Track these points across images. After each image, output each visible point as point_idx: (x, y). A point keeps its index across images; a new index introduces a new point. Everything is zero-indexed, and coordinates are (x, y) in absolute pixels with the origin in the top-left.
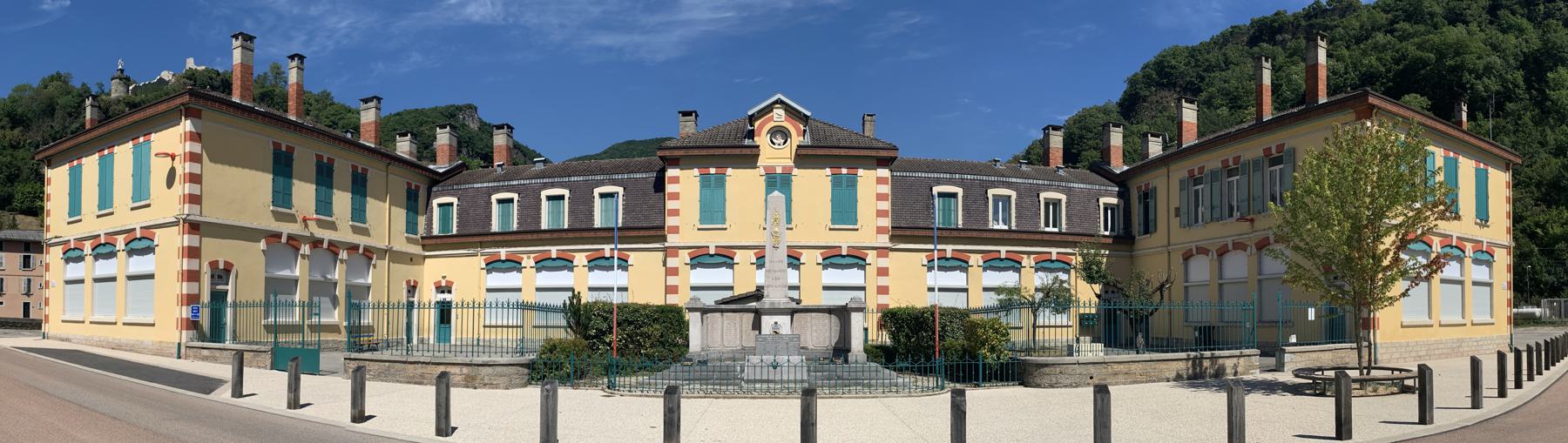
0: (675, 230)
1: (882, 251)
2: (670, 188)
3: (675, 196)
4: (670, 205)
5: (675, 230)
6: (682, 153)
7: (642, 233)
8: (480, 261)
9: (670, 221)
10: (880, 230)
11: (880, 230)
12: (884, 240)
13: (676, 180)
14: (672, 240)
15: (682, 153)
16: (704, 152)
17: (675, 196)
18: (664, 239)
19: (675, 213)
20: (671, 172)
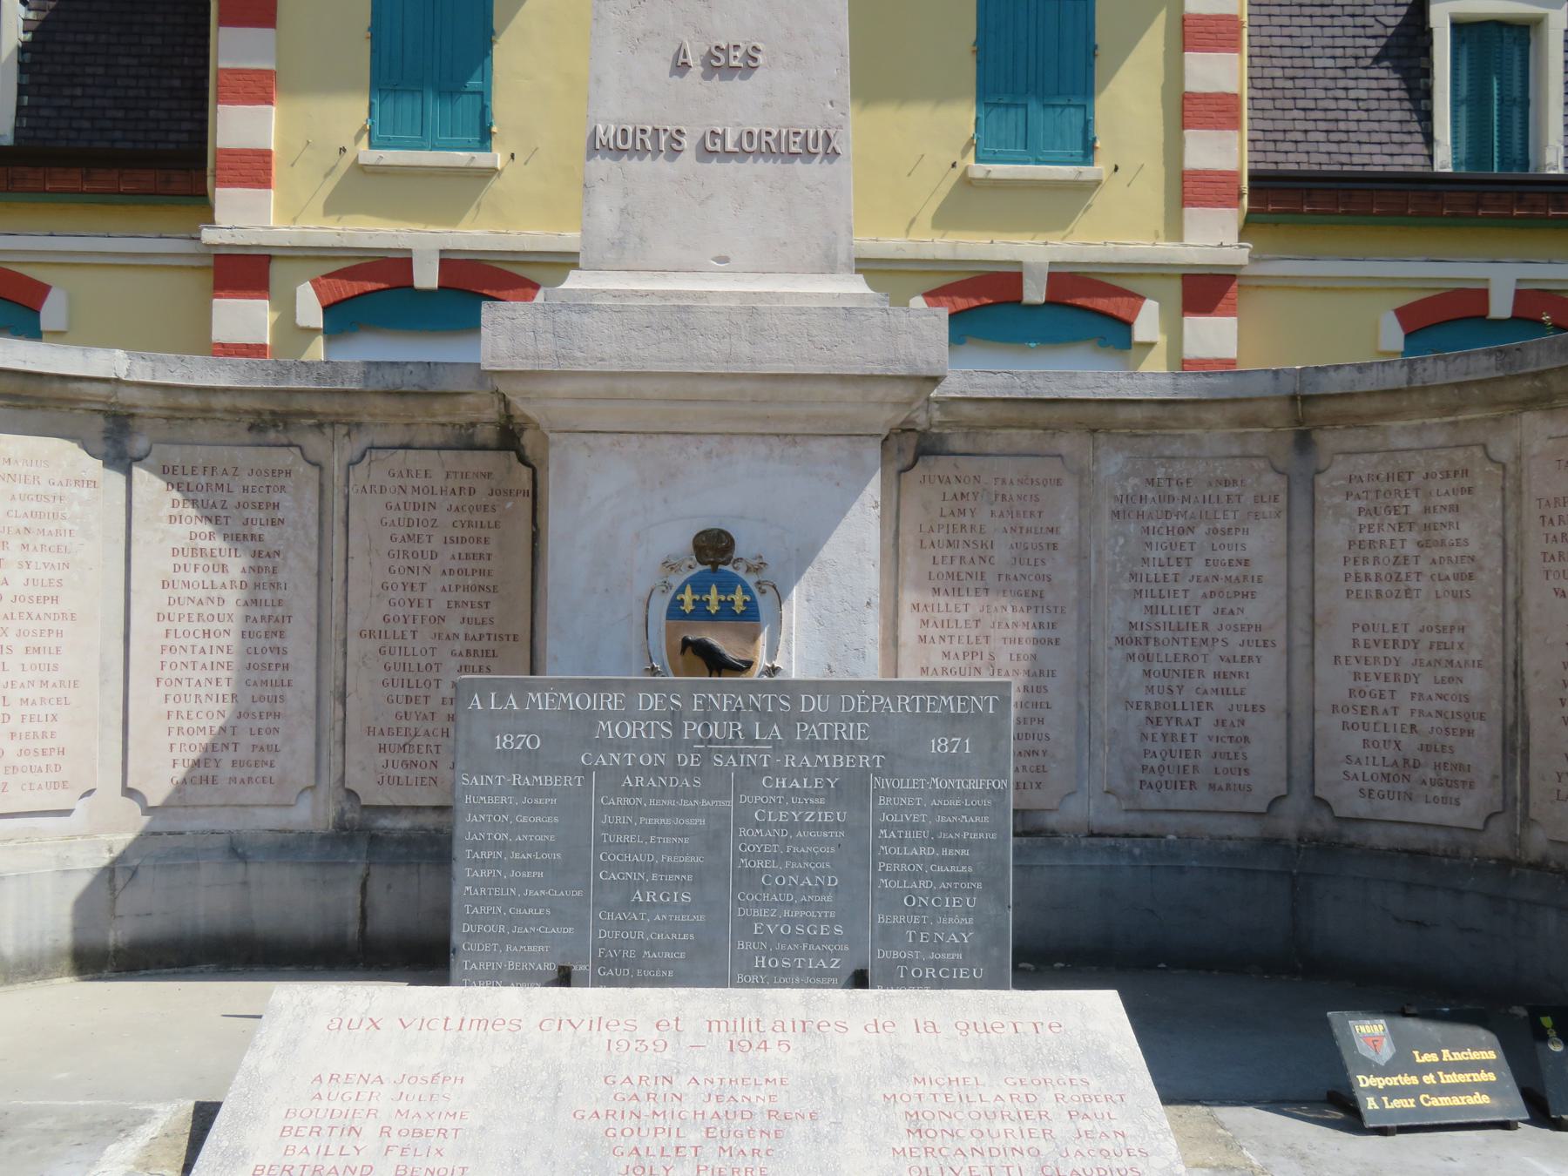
0: (254, 169)
1: (1204, 291)
5: (254, 169)
9: (233, 126)
10: (1193, 190)
11: (1193, 190)
12: (1215, 237)
14: (239, 218)
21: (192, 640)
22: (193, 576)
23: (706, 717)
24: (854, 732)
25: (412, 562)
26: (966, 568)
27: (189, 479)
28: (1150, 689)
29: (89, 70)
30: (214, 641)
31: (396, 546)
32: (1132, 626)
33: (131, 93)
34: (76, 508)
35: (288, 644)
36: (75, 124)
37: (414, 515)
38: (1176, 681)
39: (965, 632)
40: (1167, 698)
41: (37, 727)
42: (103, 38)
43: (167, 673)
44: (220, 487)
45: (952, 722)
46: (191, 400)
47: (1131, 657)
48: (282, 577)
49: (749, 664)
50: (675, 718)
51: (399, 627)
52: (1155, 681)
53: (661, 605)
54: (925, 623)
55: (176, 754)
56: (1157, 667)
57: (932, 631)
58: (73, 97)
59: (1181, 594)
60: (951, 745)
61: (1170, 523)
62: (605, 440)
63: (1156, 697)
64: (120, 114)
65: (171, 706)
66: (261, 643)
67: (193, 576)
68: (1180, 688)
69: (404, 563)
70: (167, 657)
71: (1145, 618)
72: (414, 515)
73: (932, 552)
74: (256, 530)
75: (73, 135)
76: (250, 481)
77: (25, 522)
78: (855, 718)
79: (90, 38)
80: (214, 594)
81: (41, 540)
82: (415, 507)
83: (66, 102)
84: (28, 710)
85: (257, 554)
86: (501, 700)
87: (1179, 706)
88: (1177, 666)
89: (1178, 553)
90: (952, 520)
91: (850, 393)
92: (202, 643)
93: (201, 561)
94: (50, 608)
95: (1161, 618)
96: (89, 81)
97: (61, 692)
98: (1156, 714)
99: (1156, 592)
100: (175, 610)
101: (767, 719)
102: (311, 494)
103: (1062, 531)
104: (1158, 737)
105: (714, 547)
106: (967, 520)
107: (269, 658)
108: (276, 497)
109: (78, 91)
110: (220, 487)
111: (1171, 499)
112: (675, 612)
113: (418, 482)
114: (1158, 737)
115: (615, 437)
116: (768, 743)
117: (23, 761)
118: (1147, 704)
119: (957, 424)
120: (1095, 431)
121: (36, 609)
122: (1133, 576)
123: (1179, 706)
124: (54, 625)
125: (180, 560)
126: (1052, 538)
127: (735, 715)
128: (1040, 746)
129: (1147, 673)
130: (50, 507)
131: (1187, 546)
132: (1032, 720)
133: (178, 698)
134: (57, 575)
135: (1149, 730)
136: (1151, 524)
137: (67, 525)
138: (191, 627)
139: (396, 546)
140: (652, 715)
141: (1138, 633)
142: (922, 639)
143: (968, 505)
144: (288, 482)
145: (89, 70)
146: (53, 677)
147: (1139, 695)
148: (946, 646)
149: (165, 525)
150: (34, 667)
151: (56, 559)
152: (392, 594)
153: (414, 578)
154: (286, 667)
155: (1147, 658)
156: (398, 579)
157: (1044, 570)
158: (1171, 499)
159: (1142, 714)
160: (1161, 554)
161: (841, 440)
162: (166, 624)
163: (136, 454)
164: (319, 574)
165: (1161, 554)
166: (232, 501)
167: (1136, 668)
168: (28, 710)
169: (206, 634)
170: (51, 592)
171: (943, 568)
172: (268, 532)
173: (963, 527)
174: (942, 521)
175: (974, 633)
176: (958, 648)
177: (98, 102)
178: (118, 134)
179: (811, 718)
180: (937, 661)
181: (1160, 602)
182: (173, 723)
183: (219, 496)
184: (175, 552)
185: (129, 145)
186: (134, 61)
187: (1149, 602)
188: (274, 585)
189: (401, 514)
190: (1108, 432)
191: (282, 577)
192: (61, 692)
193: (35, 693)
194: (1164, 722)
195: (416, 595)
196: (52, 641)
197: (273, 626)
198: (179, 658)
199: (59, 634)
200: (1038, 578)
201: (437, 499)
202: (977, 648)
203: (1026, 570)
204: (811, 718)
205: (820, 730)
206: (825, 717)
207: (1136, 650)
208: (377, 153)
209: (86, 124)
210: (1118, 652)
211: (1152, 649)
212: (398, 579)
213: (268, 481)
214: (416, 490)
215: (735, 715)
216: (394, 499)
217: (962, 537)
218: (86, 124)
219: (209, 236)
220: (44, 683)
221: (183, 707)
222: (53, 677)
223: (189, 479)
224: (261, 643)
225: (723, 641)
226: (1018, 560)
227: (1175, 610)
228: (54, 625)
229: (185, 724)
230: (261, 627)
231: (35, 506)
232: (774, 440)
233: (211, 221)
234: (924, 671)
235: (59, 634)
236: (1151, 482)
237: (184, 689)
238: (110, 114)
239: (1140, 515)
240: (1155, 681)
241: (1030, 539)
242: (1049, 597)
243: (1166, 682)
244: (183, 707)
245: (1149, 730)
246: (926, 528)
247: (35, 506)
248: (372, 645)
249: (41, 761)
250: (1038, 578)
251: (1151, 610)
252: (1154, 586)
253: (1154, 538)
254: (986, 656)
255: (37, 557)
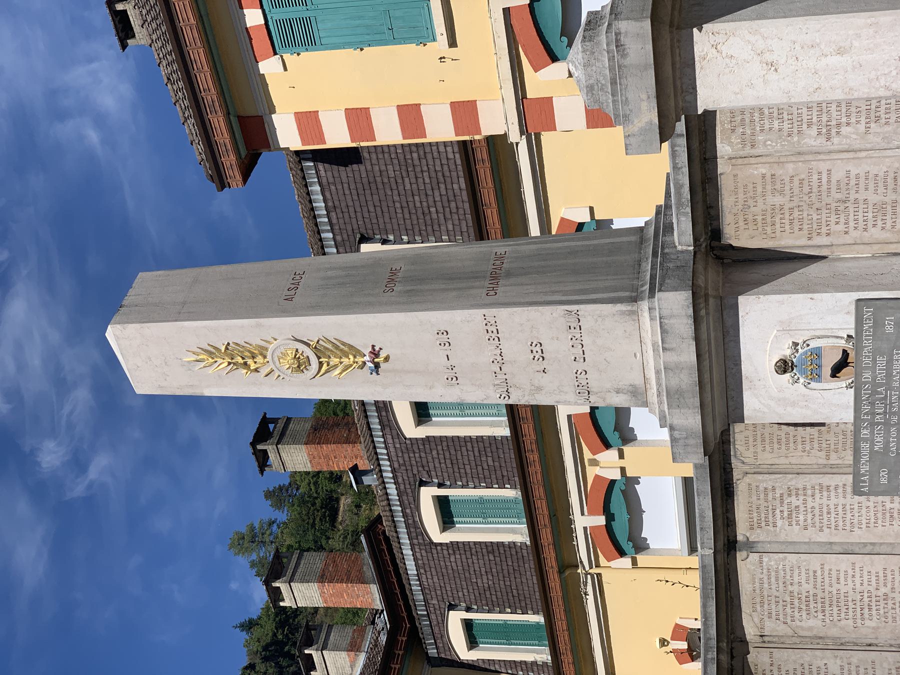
0: (465, 112)
2: (337, 136)
3: (358, 118)
4: (388, 132)
5: (465, 112)
6: (218, 122)
7: (488, 194)
8: (616, 573)
9: (440, 128)
13: (308, 122)
14: (497, 119)
15: (218, 122)
16: (198, 55)
17: (358, 118)
18: (498, 145)
19: (410, 116)
20: (288, 135)
21: (832, 518)
22: (801, 518)
23: (873, 414)
24: (882, 361)
25: (792, 440)
26: (787, 216)
27: (755, 520)
28: (858, 122)
29: (418, 204)
30: (832, 510)
31: (783, 447)
32: (819, 134)
33: (427, 180)
34: (772, 563)
35: (833, 484)
36: (454, 210)
37: (767, 441)
38: (853, 109)
39: (824, 215)
40: (864, 113)
41: (874, 579)
42: (396, 198)
43: (848, 528)
44: (758, 508)
45: (878, 324)
46: (720, 522)
47: (838, 133)
48: (800, 486)
49: (845, 351)
50: (873, 424)
51: (824, 445)
52: (853, 120)
53: (813, 385)
54: (819, 234)
55: (887, 524)
56: (844, 120)
57: (824, 230)
58: (437, 212)
59: (800, 111)
60: (889, 324)
61: (757, 120)
62: (730, 403)
63: (863, 119)
64: (442, 186)
65: (864, 526)
66: (833, 494)
67: (801, 518)
68: (857, 107)
69: (792, 445)
70: (840, 528)
71: (815, 127)
72: (767, 441)
73: (778, 234)
74: (778, 495)
75: (461, 211)
76: (754, 498)
77: (781, 584)
78: (874, 361)
79: (398, 205)
80: (809, 510)
81: (788, 577)
82: (763, 440)
83: (441, 216)
84: (865, 583)
85: (790, 495)
86: (864, 482)
87: (868, 107)
88: (844, 110)
89: (775, 114)
90: (760, 224)
91: (704, 327)
92: (833, 515)
93: (794, 515)
94: (819, 573)
95: (815, 119)
96: (425, 204)
97: (857, 569)
98: (873, 118)
99: (799, 123)
100: (818, 524)
101: (874, 392)
102: (760, 477)
103: (764, 171)
104: (887, 116)
105: (784, 366)
106: (759, 218)
107: (840, 490)
108: (761, 488)
109: (433, 210)
110: (758, 508)
111: (743, 120)
112: (818, 377)
113: (751, 440)
114: (887, 116)
115: (729, 400)
116: (886, 392)
117: (889, 585)
118: (867, 123)
119: (706, 226)
120: (705, 159)
121: (819, 580)
122: (789, 135)
123: (868, 107)
124: (826, 573)
125: (794, 523)
126: (768, 176)
127: (872, 404)
128: (891, 175)
129: (848, 124)
130: (773, 574)
131: (771, 111)
132: (875, 180)
133: (860, 523)
134: (803, 570)
135: (883, 121)
136: (758, 129)
137: (781, 567)
138: (826, 519)
139: (783, 447)
140: (872, 433)
141: (824, 130)
142: (828, 234)
143: (750, 217)
144: (754, 485)
145: (418, 204)
146: (850, 572)
147: (862, 127)
148: (832, 223)
149: (778, 529)
150: (846, 580)
151: (796, 572)
152: (808, 448)
153: (800, 440)
154: (845, 485)
155: (839, 125)
156: (800, 447)
157: (787, 179)
158: (743, 120)
159: (873, 125)
160: (776, 124)
161: (725, 313)
162: (825, 528)
163: (745, 539)
164: (798, 474)
165: (776, 124)
166: (766, 504)
167: (845, 130)
168: (865, 583)
169: (829, 513)
170: (811, 574)
171: (787, 227)
172: (778, 493)
173: (763, 219)
174: (760, 229)
175: (824, 211)
176: (833, 218)
177: (438, 199)
178: (456, 186)
179: (874, 378)
180: (841, 227)
181: (805, 121)
182: (872, 525)
183: (762, 508)
184: (790, 525)
185: (462, 180)
186: (407, 180)
187: (805, 126)
188: (805, 489)
189: (767, 446)
190: (705, 153)
191: (800, 486)
192: (857, 569)
193: (858, 581)
194: (878, 114)
195: (808, 440)
196: (834, 573)
197: (825, 489)
198: (841, 524)
199: (830, 570)
200: (791, 181)
201: (759, 433)
202: (833, 209)
203: (787, 188)
204: (874, 378)
205: (880, 374)
206: (874, 372)
207: (834, 131)
208: (438, 37)
209: (453, 205)
210: (836, 140)
211: (834, 123)
212: (800, 447)
213: (754, 491)
214: (755, 441)
215: (872, 404)
216: (759, 448)
217: (769, 220)
218: (453, 205)
219: (514, 136)
220: (853, 576)
221: (864, 522)
222: (850, 572)
223: (755, 520)
224: (833, 494)
225: (831, 359)
226: (782, 193)
227: (810, 113)
228: (826, 573)
229: (873, 520)
230: (825, 494)
231: (773, 580)
232: (726, 340)
233: (505, 136)
234: (846, 233)
235: (830, 570)
236: (733, 131)
237: (856, 521)
238: (444, 192)
239: (753, 134)
240: (853, 120)
241: (769, 187)
242: (803, 176)
243: (854, 115)
244: (864, 522)
245: (883, 121)
246: (765, 236)
247: (773, 580)
248: (833, 456)
249: (890, 577)
250: (791, 181)
251: (809, 126)
252: (795, 125)
253: (767, 127)
254: (838, 204)
255: (796, 579)
